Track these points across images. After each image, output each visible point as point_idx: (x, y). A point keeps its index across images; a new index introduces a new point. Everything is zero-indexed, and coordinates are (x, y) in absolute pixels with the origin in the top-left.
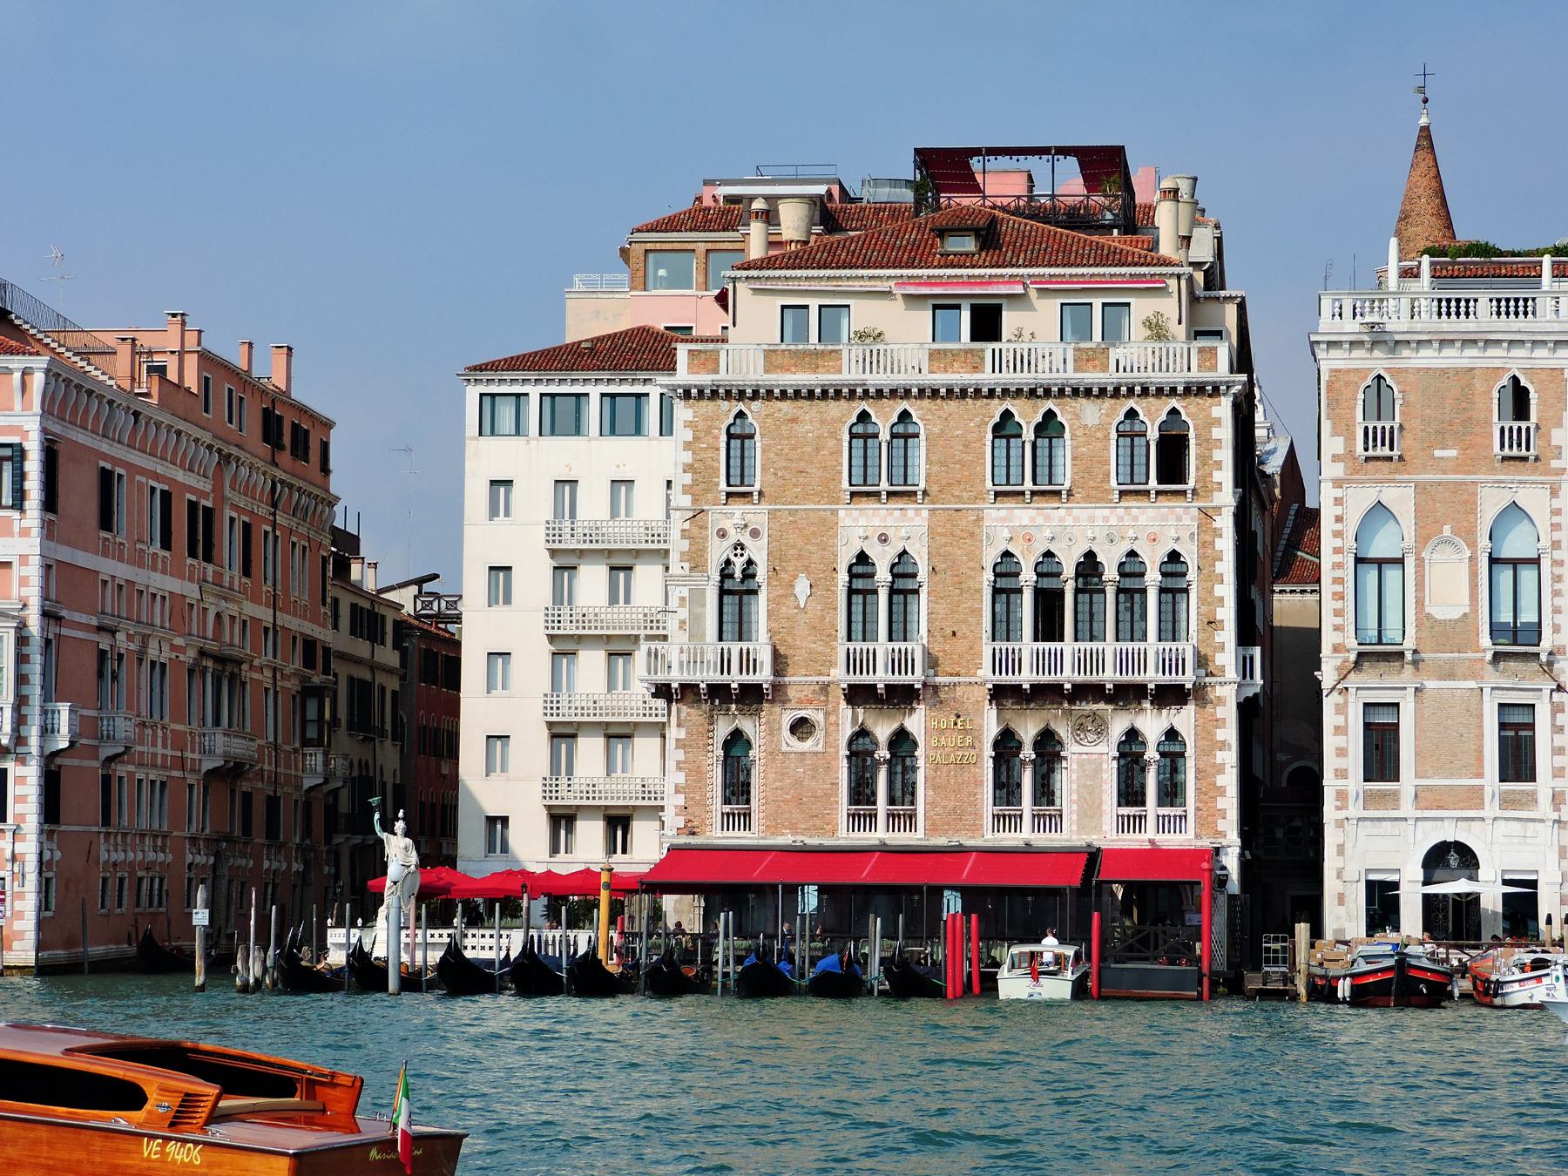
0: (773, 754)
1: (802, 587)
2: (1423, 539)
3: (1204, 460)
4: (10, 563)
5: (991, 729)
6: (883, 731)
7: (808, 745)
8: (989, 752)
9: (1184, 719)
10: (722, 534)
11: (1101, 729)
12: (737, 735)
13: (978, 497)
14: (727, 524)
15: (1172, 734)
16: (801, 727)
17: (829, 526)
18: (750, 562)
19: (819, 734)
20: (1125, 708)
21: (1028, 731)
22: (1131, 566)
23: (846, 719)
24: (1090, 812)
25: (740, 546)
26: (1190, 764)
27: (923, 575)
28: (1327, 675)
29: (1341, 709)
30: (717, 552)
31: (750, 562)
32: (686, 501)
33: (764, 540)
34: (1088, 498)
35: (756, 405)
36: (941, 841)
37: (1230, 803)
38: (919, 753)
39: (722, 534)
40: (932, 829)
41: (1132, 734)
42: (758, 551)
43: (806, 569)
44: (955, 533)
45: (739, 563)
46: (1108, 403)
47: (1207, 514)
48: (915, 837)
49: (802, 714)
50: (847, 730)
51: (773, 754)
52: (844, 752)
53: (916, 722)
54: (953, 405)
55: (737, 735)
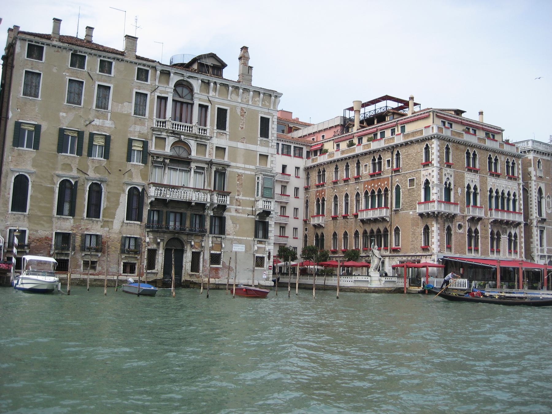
0: (455, 232)
1: (459, 190)
2: (546, 195)
3: (518, 173)
4: (267, 156)
5: (490, 231)
6: (473, 229)
7: (461, 231)
8: (490, 236)
9: (517, 231)
10: (445, 175)
11: (506, 233)
13: (486, 174)
14: (446, 173)
15: (515, 234)
16: (460, 227)
17: (463, 177)
18: (450, 183)
19: (463, 229)
20: (509, 227)
21: (495, 232)
22: (509, 194)
23: (467, 226)
24: (504, 252)
25: (448, 178)
26: (518, 241)
27: (478, 191)
28: (535, 223)
29: (537, 231)
30: (444, 180)
31: (450, 183)
32: (438, 165)
33: (453, 176)
34: (503, 178)
35: (451, 144)
36: (483, 257)
37: (523, 250)
38: (479, 234)
39: (445, 175)
40: (481, 254)
41: (510, 235)
42: (452, 180)
43: (460, 187)
44: (483, 182)
45: (448, 182)
46: (505, 156)
47: (519, 184)
48: (479, 256)
49: (460, 223)
50: (467, 229)
51: (455, 232)
52: (467, 234)
53: (479, 228)
54: (482, 151)
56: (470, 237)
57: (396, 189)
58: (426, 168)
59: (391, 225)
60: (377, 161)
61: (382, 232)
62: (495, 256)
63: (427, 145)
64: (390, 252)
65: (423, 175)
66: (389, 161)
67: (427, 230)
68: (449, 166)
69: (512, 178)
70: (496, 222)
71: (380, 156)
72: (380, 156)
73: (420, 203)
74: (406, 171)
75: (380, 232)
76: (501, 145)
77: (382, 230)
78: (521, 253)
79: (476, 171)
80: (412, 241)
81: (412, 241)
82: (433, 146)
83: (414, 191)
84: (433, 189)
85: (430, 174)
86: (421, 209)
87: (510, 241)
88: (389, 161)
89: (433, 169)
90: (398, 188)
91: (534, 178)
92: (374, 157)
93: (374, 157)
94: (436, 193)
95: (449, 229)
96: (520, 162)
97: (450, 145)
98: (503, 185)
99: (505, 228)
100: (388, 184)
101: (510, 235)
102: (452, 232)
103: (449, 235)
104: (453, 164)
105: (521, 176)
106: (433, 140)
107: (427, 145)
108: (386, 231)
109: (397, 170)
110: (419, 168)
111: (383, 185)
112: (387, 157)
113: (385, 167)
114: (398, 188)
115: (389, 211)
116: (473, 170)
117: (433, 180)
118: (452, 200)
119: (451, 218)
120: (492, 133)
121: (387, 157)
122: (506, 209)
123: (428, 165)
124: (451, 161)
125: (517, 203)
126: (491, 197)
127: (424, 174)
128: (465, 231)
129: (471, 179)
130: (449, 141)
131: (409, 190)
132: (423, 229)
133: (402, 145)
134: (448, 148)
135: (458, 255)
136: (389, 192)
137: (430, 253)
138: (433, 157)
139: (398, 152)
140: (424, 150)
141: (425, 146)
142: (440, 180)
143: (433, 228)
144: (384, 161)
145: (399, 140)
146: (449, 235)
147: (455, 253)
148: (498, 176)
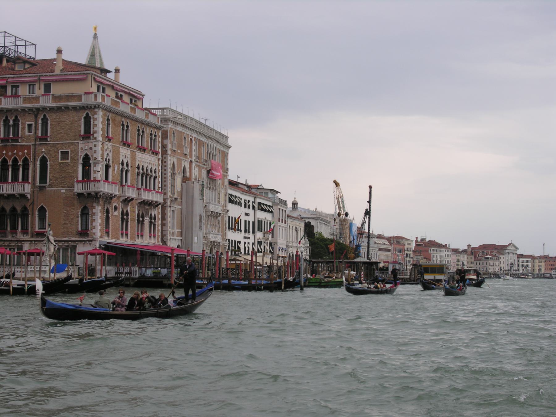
0: (112, 215)
12: (107, 209)
16: (116, 208)
17: (119, 152)
25: (108, 154)
26: (156, 223)
37: (160, 234)
44: (133, 158)
47: (159, 159)
51: (112, 215)
54: (133, 122)
55: (107, 209)
56: (122, 219)
57: (41, 161)
58: (86, 141)
59: (33, 204)
60: (11, 123)
61: (8, 211)
62: (138, 241)
63: (87, 114)
64: (32, 237)
65: (82, 149)
66: (30, 126)
67: (85, 213)
68: (109, 140)
69: (155, 153)
70: (144, 203)
71: (16, 117)
72: (16, 117)
73: (78, 182)
74: (57, 140)
75: (6, 211)
76: (147, 115)
77: (19, 209)
78: (158, 236)
79: (129, 145)
80: (64, 224)
81: (64, 224)
82: (96, 116)
83: (68, 166)
84: (95, 165)
85: (91, 148)
86: (78, 188)
87: (151, 222)
88: (30, 126)
89: (96, 143)
90: (44, 161)
91: (169, 152)
92: (7, 117)
93: (7, 117)
94: (98, 172)
95: (108, 212)
96: (160, 134)
97: (111, 115)
98: (148, 161)
99: (147, 209)
100: (29, 154)
101: (151, 218)
102: (110, 215)
103: (108, 218)
104: (112, 138)
105: (160, 150)
106: (96, 110)
107: (87, 114)
108: (25, 209)
109: (44, 138)
110: (75, 140)
111: (20, 153)
112: (30, 120)
113: (24, 131)
114: (44, 161)
115: (30, 186)
116: (127, 144)
117: (95, 155)
118: (110, 179)
119: (109, 198)
120: (135, 98)
121: (26, 121)
122: (148, 188)
123: (89, 138)
124: (110, 135)
125: (157, 181)
126: (138, 174)
127: (83, 147)
128: (119, 213)
129: (125, 153)
130: (110, 111)
131: (61, 163)
132: (80, 210)
133: (52, 109)
134: (108, 120)
135: (113, 241)
136: (31, 164)
137: (90, 239)
138: (95, 129)
139: (45, 116)
140: (83, 120)
141: (85, 115)
142: (102, 155)
143: (94, 211)
144: (23, 124)
145: (46, 102)
146: (108, 218)
147: (112, 239)
148: (144, 150)
